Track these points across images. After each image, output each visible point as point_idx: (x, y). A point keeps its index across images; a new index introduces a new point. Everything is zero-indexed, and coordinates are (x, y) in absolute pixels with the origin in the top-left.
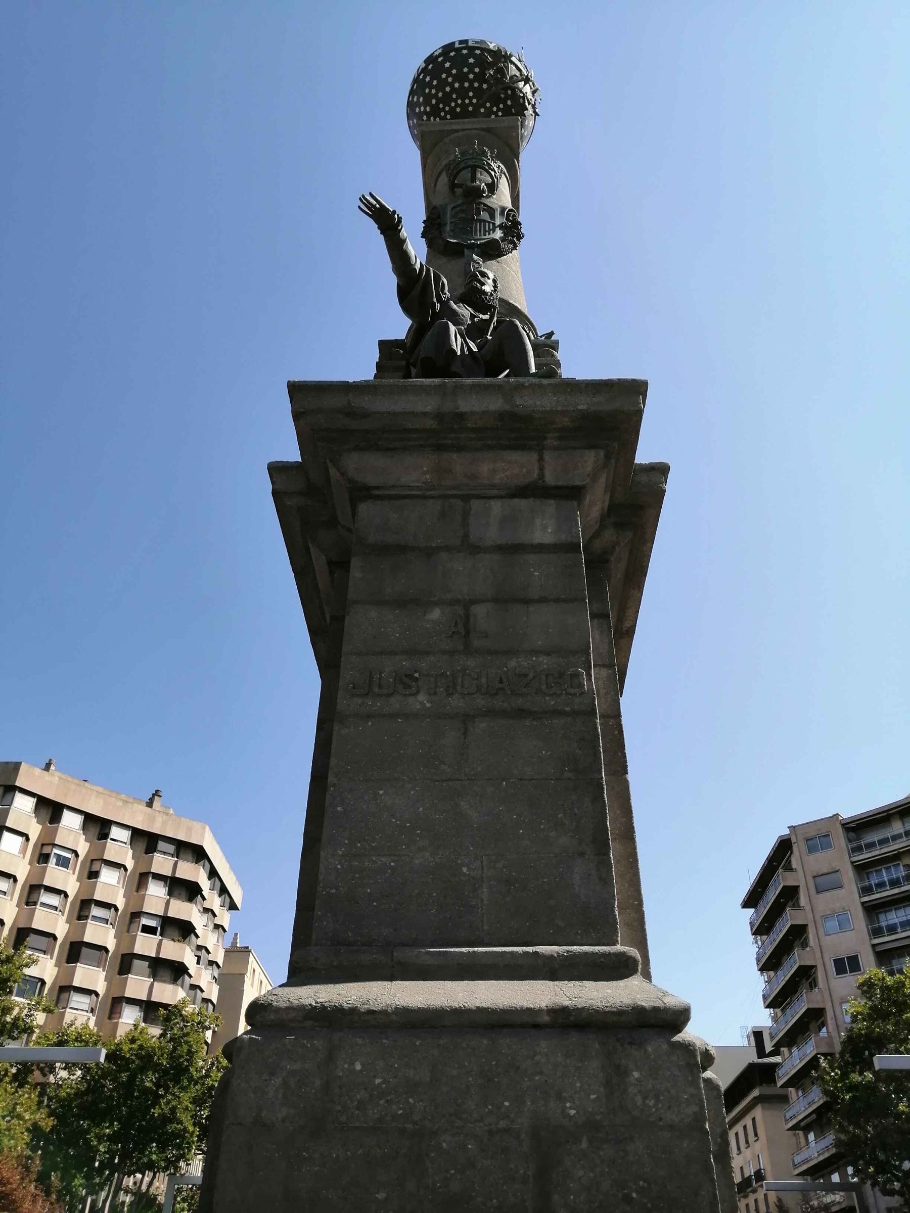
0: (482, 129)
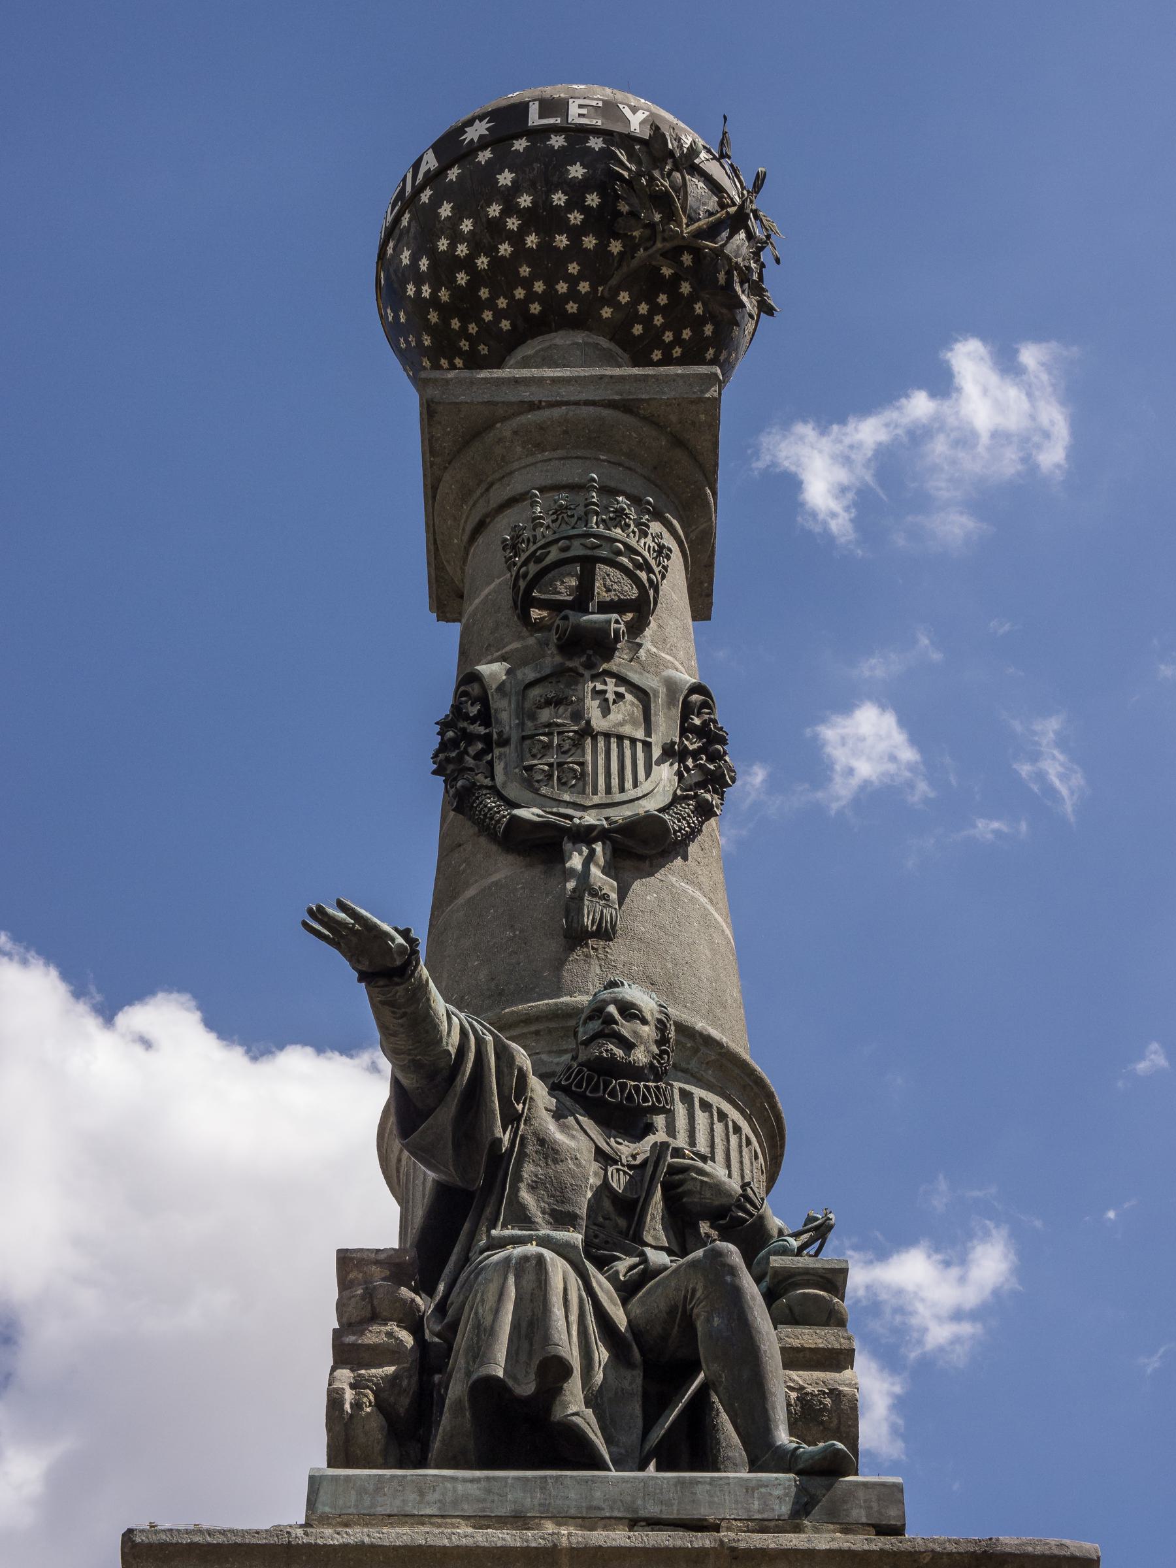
0: (611, 405)
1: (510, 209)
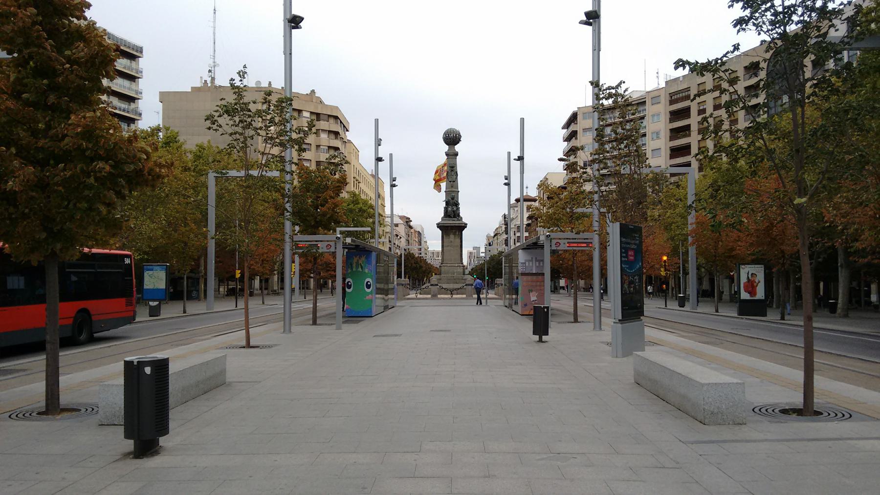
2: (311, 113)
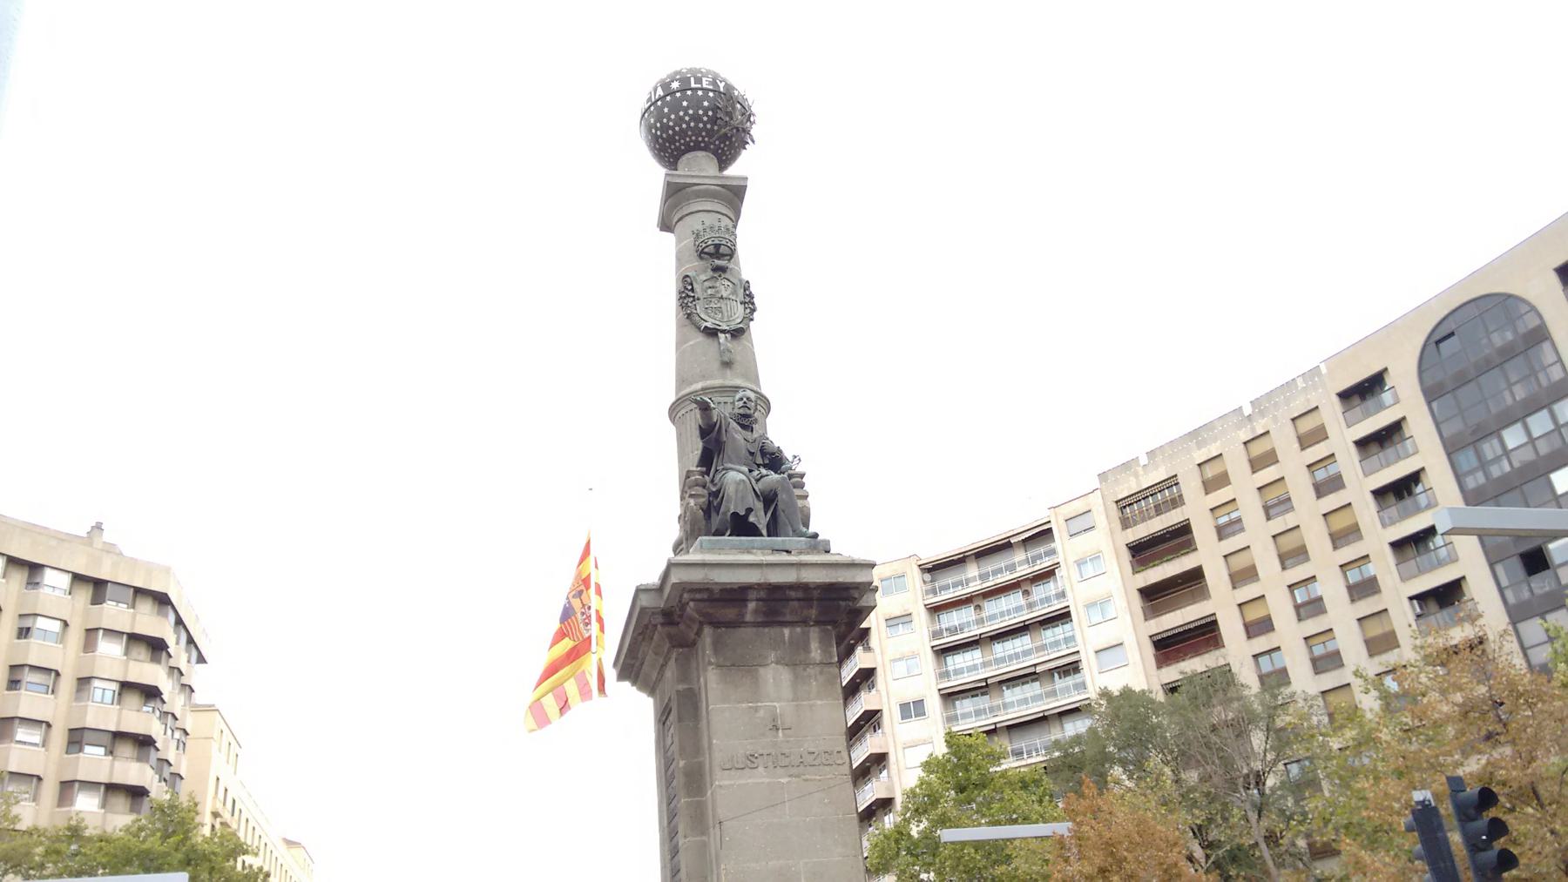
1: (686, 114)
2: (78, 578)
